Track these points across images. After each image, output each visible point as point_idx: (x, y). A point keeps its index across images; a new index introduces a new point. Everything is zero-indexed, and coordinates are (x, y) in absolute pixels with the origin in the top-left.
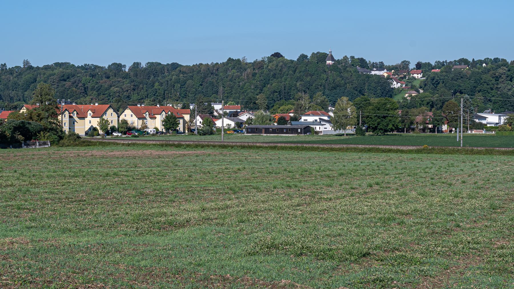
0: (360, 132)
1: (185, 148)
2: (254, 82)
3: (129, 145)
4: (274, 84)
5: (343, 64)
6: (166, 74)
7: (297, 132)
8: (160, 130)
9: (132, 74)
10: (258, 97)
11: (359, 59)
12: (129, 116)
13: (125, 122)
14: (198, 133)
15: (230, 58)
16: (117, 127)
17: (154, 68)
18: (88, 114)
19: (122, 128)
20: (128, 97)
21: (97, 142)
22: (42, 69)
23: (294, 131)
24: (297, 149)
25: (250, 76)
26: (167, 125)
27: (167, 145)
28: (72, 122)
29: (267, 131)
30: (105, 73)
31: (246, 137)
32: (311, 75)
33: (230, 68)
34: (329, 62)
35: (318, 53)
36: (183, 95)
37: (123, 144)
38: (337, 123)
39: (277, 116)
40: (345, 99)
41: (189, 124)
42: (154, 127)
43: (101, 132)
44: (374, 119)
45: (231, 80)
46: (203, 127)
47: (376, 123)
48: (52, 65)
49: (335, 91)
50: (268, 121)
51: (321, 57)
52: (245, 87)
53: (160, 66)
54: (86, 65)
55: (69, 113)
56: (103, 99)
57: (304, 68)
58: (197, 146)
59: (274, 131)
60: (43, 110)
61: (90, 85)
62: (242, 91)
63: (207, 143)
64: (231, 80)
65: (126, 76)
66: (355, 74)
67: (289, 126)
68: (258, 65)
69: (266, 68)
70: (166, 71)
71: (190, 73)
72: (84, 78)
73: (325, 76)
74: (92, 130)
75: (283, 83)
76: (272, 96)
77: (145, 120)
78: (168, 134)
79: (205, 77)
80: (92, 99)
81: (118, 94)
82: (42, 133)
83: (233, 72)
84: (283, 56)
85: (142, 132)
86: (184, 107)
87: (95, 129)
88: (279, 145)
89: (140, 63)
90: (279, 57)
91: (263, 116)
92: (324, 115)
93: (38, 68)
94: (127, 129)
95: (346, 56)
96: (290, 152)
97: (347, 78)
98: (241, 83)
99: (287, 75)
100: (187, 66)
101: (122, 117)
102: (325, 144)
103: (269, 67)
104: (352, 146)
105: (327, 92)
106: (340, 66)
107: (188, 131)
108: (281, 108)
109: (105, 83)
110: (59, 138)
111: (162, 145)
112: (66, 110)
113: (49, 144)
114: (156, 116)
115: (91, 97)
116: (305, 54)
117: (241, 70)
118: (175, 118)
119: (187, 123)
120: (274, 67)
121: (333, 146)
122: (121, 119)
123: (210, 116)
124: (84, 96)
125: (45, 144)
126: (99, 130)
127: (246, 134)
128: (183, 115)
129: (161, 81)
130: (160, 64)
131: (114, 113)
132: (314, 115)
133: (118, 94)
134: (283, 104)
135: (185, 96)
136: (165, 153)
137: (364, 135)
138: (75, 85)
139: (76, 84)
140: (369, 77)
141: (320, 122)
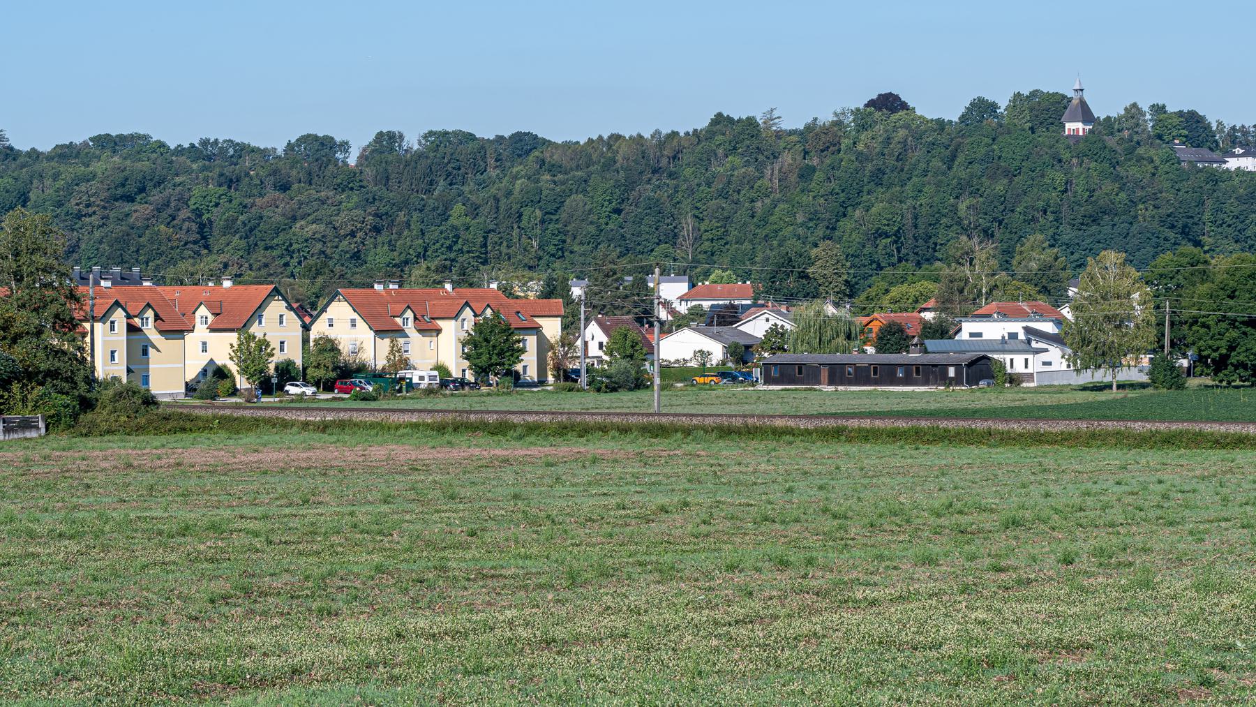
0: (1166, 376)
1: (520, 438)
2: (806, 199)
3: (324, 427)
4: (878, 208)
5: (1126, 133)
6: (493, 173)
7: (943, 379)
8: (456, 373)
9: (369, 172)
10: (814, 252)
11: (1180, 114)
12: (343, 326)
13: (329, 346)
14: (589, 384)
15: (720, 115)
16: (299, 363)
17: (448, 150)
18: (198, 320)
19: (318, 366)
20: (356, 256)
21: (215, 417)
22: (49, 157)
23: (931, 373)
24: (917, 436)
25: (793, 178)
26: (479, 356)
27: (456, 429)
28: (139, 350)
29: (838, 374)
30: (275, 172)
31: (760, 397)
32: (1011, 175)
33: (720, 151)
34: (1075, 127)
35: (1034, 93)
36: (551, 249)
37: (306, 425)
38: (1088, 346)
39: (880, 319)
40: (1112, 257)
41: (560, 351)
42: (433, 362)
43: (242, 383)
44: (1213, 331)
45: (723, 194)
46: (610, 364)
47: (1223, 343)
48: (86, 144)
49: (1094, 228)
50: (841, 340)
51: (1046, 110)
52: (772, 219)
53: (471, 145)
54: (205, 143)
55: (129, 317)
56: (266, 265)
57: (983, 150)
58: (563, 430)
59: (864, 375)
60: (23, 306)
61: (217, 216)
62: (762, 233)
63: (599, 419)
64: (723, 194)
65: (350, 181)
66: (1166, 167)
67: (914, 356)
68: (820, 140)
69: (849, 149)
70: (491, 162)
71: (578, 167)
72: (197, 191)
73: (1060, 178)
74: (210, 374)
75: (910, 202)
76: (869, 248)
77: (401, 341)
78: (484, 389)
79: (630, 185)
80: (226, 266)
81: (319, 246)
82: (15, 387)
83: (731, 166)
84: (911, 105)
85: (391, 381)
86: (548, 293)
87: (221, 373)
88: (853, 423)
89: (401, 136)
90: (893, 110)
91: (827, 321)
92: (1042, 316)
93: (34, 155)
94: (339, 374)
95: (1134, 105)
96: (890, 448)
97: (1138, 183)
98: (759, 204)
99: (925, 173)
100: (567, 145)
101: (319, 329)
102: (1045, 418)
103: (860, 147)
104: (1110, 425)
105: (1068, 234)
106: (1111, 142)
107: (557, 377)
108: (895, 291)
109: (271, 205)
110: (79, 401)
111: (441, 428)
112: (117, 304)
113: (41, 425)
114: (441, 323)
115: (223, 258)
116: (990, 98)
117: (761, 157)
118: (508, 331)
119: (552, 347)
120: (877, 146)
121: (1043, 427)
122: (313, 334)
123: (638, 319)
124: (198, 253)
125: (27, 425)
126: (238, 377)
127: (761, 387)
128: (540, 321)
129: (473, 198)
130: (471, 137)
131: (290, 316)
132: (1005, 316)
133: (319, 246)
134: (903, 280)
135: (561, 252)
136: (442, 454)
137: (1181, 387)
138: (164, 215)
139: (169, 211)
140: (1216, 179)
141: (1029, 342)
